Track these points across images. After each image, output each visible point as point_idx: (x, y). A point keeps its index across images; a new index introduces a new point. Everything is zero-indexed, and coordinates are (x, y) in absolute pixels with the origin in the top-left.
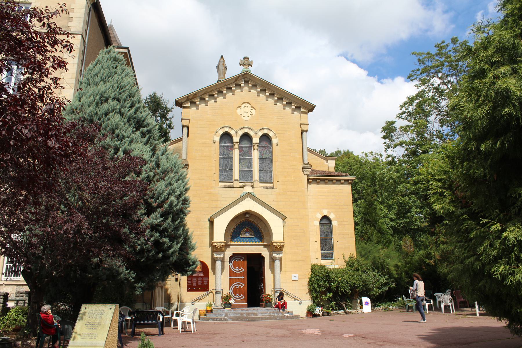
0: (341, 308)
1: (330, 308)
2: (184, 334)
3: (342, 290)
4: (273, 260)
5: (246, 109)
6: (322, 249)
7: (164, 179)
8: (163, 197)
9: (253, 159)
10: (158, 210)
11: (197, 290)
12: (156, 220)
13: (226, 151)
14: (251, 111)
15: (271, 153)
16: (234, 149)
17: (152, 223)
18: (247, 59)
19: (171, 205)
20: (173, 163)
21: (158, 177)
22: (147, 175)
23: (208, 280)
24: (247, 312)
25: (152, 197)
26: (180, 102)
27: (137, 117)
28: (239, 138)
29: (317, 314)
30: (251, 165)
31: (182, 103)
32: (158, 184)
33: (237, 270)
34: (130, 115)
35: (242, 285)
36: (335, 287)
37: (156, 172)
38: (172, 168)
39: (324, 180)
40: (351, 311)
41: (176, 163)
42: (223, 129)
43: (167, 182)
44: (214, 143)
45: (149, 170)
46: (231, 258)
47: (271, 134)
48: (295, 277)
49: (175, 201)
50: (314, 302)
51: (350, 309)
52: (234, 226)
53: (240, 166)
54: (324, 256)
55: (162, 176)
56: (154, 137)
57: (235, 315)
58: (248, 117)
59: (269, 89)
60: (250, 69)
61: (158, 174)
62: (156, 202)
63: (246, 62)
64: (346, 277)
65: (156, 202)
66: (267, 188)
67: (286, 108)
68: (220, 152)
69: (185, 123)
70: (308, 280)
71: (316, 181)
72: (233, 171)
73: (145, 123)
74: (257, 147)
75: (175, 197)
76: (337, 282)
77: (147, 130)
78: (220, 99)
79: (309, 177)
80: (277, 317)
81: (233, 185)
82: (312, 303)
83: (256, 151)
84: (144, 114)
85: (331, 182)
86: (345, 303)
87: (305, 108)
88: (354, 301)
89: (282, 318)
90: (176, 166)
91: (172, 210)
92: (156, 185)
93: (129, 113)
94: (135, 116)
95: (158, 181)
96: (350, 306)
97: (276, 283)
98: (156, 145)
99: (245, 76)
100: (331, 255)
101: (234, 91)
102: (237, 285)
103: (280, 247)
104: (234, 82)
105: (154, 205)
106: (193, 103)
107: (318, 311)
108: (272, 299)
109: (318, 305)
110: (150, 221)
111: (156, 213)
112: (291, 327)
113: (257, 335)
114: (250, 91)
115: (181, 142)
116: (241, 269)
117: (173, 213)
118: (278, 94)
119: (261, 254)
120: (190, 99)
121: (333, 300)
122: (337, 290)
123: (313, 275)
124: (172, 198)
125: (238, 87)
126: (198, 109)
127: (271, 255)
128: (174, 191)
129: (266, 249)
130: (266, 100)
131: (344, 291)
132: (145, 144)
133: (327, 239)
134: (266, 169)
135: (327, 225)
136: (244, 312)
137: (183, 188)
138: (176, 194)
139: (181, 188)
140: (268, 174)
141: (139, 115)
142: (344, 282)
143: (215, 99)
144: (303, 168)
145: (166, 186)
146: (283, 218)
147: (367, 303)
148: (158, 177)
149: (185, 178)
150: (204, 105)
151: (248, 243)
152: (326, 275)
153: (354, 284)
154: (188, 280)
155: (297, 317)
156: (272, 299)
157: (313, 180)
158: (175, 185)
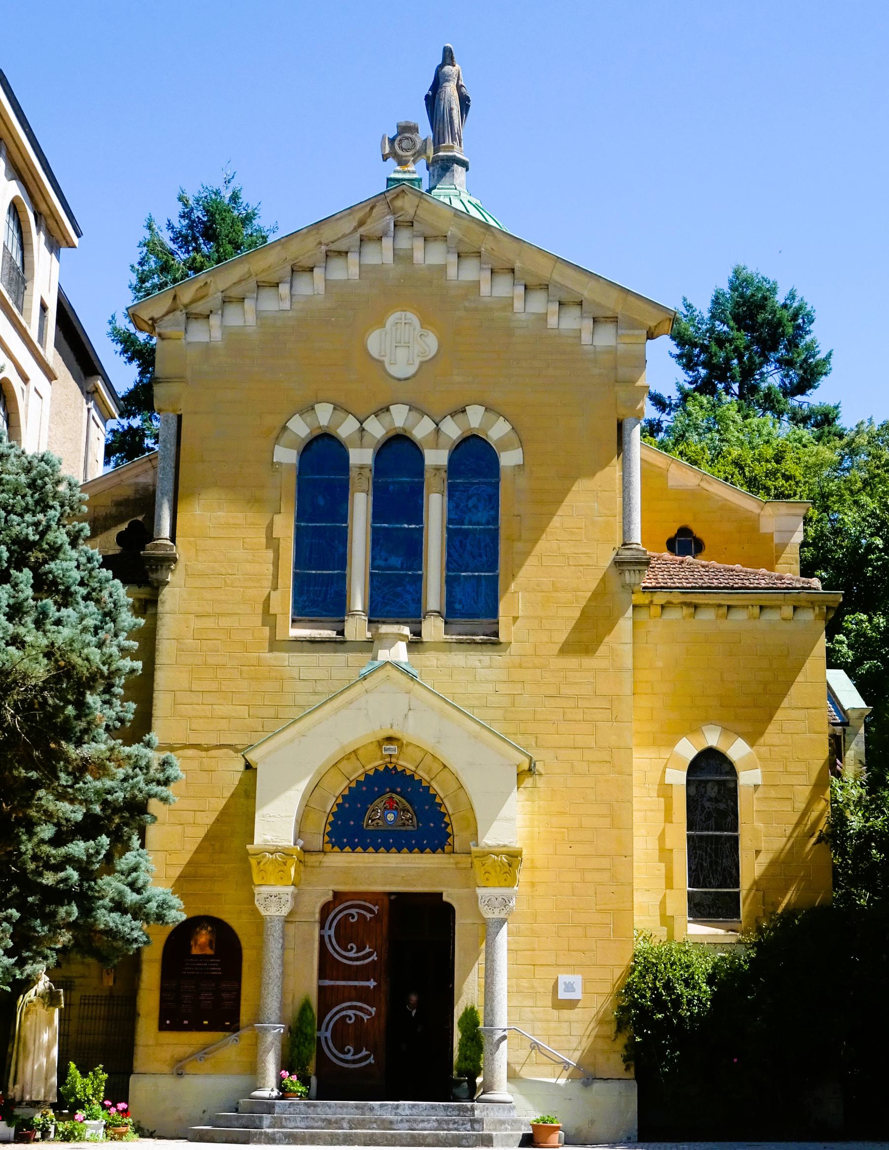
33: (352, 954)
48: (569, 988)
102: (350, 1013)
104: (355, 229)
116: (368, 950)
119: (441, 894)
120: (186, 306)
132: (17, 488)
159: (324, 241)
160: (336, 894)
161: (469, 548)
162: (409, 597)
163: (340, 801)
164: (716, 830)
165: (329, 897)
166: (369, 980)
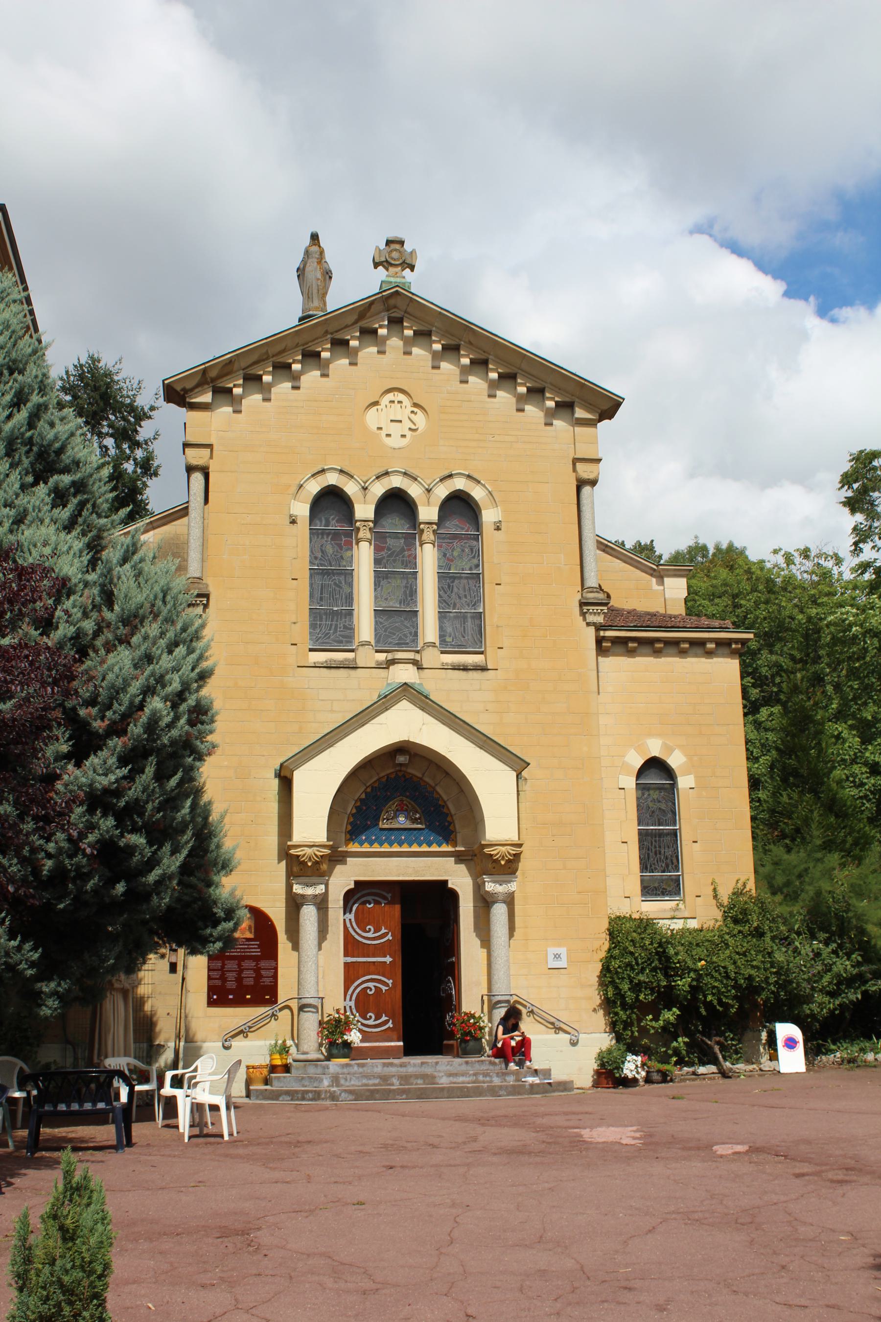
0: (708, 1058)
1: (671, 1056)
2: (197, 1145)
3: (709, 998)
4: (485, 902)
5: (396, 412)
6: (645, 865)
7: (129, 643)
8: (125, 699)
9: (419, 575)
10: (111, 743)
11: (239, 1001)
12: (106, 775)
13: (329, 550)
14: (412, 416)
15: (476, 553)
16: (357, 543)
17: (91, 785)
18: (397, 246)
19: (152, 726)
20: (157, 588)
21: (110, 636)
22: (72, 629)
23: (276, 969)
24: (403, 1070)
25: (92, 702)
26: (178, 388)
27: (36, 439)
28: (372, 507)
29: (630, 1076)
30: (411, 595)
31: (186, 391)
32: (111, 659)
33: (370, 935)
34: (12, 431)
35: (387, 985)
36: (687, 988)
37: (103, 620)
38: (153, 605)
39: (651, 642)
40: (741, 1066)
41: (169, 589)
42: (320, 478)
43: (138, 653)
44: (293, 522)
45: (79, 615)
46: (349, 897)
47: (477, 493)
48: (557, 957)
49: (165, 713)
50: (619, 1038)
51: (737, 1061)
52: (359, 792)
53: (376, 597)
54: (649, 890)
55: (122, 631)
56: (94, 506)
57: (365, 1081)
58: (403, 436)
59: (470, 343)
60: (408, 279)
61: (109, 625)
62: (102, 719)
63: (395, 255)
64: (722, 958)
65: (103, 718)
66: (465, 668)
67: (528, 408)
68: (312, 551)
69: (197, 457)
70: (599, 966)
71: (624, 647)
72: (355, 613)
73: (66, 458)
74: (432, 537)
75: (165, 699)
76: (692, 974)
77: (74, 483)
78: (311, 378)
79: (602, 633)
80: (501, 1087)
81: (355, 660)
82: (614, 1041)
83: (428, 548)
84: (62, 429)
85: (672, 650)
86: (718, 1043)
87: (588, 407)
88: (749, 1035)
89: (517, 1090)
90: (168, 598)
91: (155, 741)
92: (103, 662)
93: (10, 424)
94: (29, 434)
95: (110, 648)
96: (737, 1052)
97: (495, 978)
98: (101, 530)
99: (392, 302)
100: (673, 885)
101: (356, 351)
102: (371, 985)
103: (509, 861)
104: (356, 322)
105: (98, 725)
106: (223, 393)
107: (633, 1067)
108: (481, 1029)
109: (633, 1048)
110: (84, 780)
111: (104, 754)
112: (544, 1121)
113: (433, 1146)
114: (408, 353)
115: (184, 520)
116: (383, 931)
117: (158, 751)
118: (500, 361)
119: (446, 882)
120: (213, 380)
121: (680, 1032)
122: (695, 999)
123: (616, 952)
124: (156, 703)
125: (368, 338)
126: (240, 412)
127: (478, 888)
128: (161, 680)
129: (462, 867)
130: (462, 382)
131: (715, 1002)
133: (660, 834)
134: (462, 607)
135: (660, 788)
136: (393, 1070)
137: (193, 670)
138: (169, 689)
139: (186, 669)
140: (469, 623)
141: (46, 432)
142: (716, 975)
143: (295, 378)
144: (582, 604)
145: (136, 666)
146: (519, 765)
147: (791, 1043)
148: (110, 636)
149: (196, 636)
150: (258, 397)
151: (405, 848)
152: (657, 953)
153: (750, 978)
154: (210, 969)
155: (565, 1086)
156: (481, 1029)
157: (616, 641)
158: (166, 662)
159: (331, 330)
160: (357, 883)
161: (455, 589)
162: (406, 631)
163: (358, 804)
164: (659, 825)
165: (352, 886)
166: (385, 957)
